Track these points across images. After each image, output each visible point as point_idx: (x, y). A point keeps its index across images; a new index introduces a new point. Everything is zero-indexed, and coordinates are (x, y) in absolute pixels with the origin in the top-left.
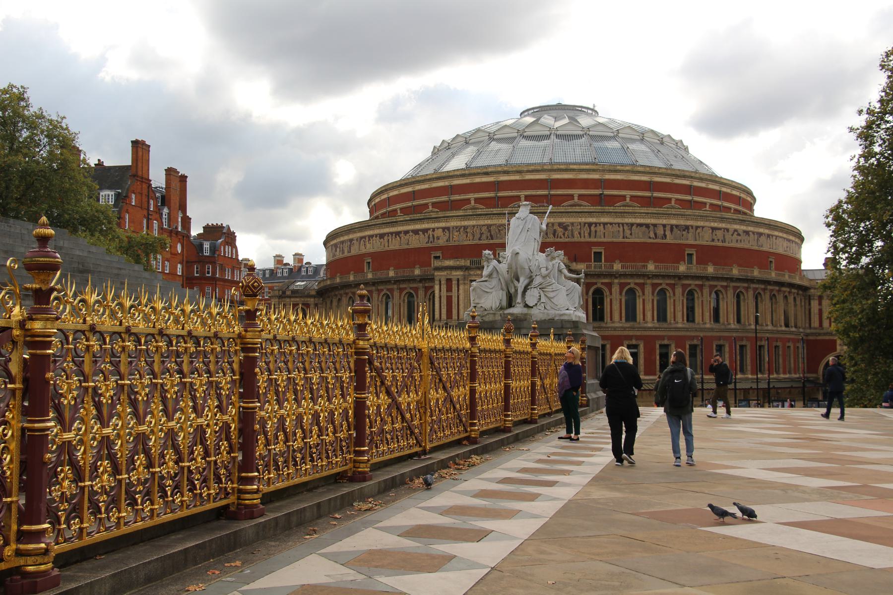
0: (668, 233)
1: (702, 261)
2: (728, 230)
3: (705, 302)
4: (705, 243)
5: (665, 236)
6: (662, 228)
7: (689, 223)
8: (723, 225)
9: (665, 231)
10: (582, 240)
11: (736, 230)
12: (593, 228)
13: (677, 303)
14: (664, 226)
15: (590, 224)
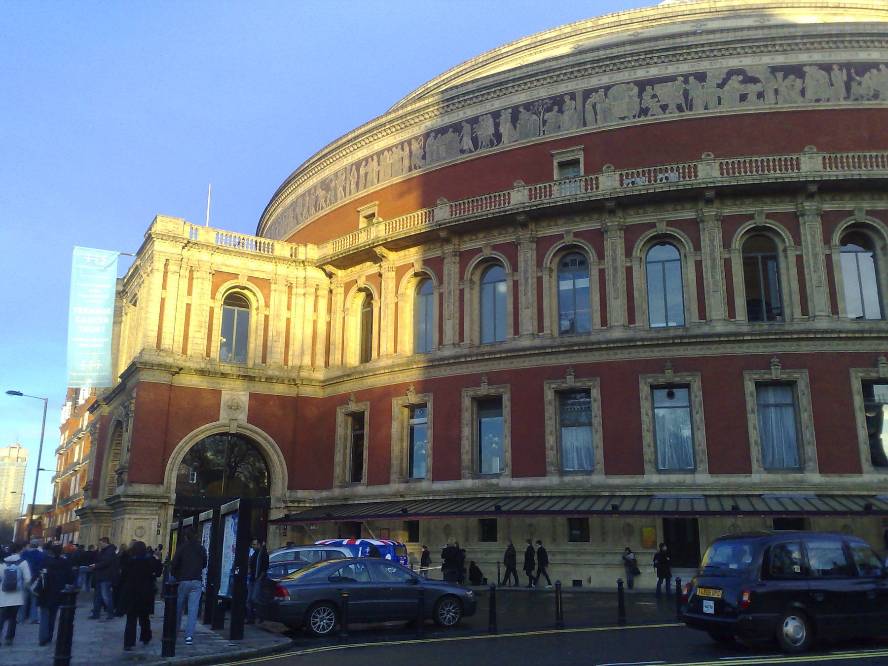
0: (505, 129)
1: (594, 168)
2: (701, 77)
3: (609, 273)
4: (614, 124)
5: (498, 136)
6: (491, 121)
7: (561, 89)
8: (685, 68)
9: (497, 126)
10: (348, 200)
11: (731, 73)
12: (362, 171)
13: (521, 288)
14: (496, 115)
15: (358, 164)
